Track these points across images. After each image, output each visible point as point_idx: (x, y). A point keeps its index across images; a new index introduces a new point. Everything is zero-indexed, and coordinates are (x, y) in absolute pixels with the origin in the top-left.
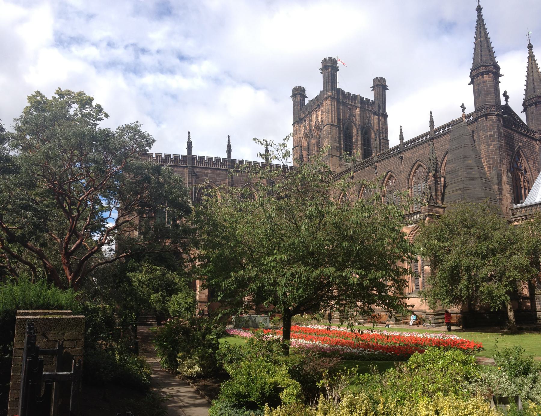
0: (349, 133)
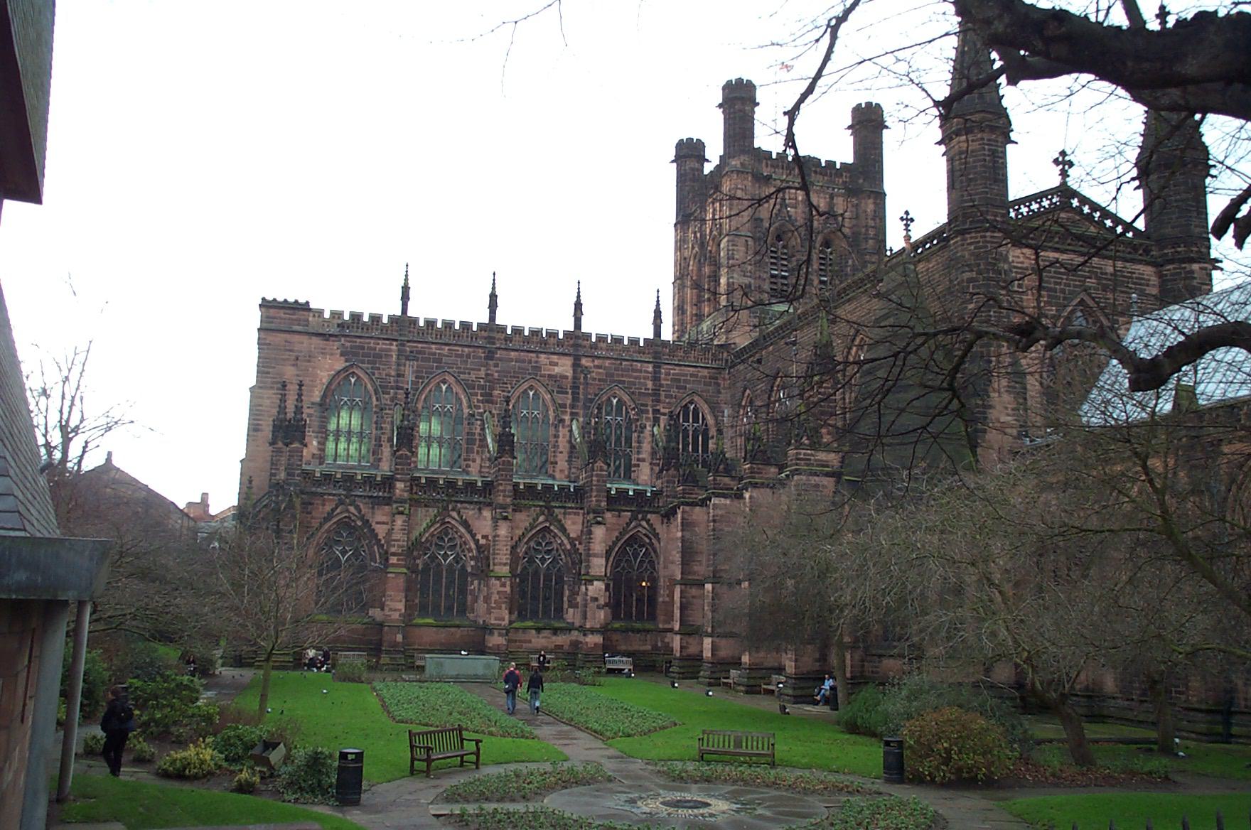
0: (784, 247)
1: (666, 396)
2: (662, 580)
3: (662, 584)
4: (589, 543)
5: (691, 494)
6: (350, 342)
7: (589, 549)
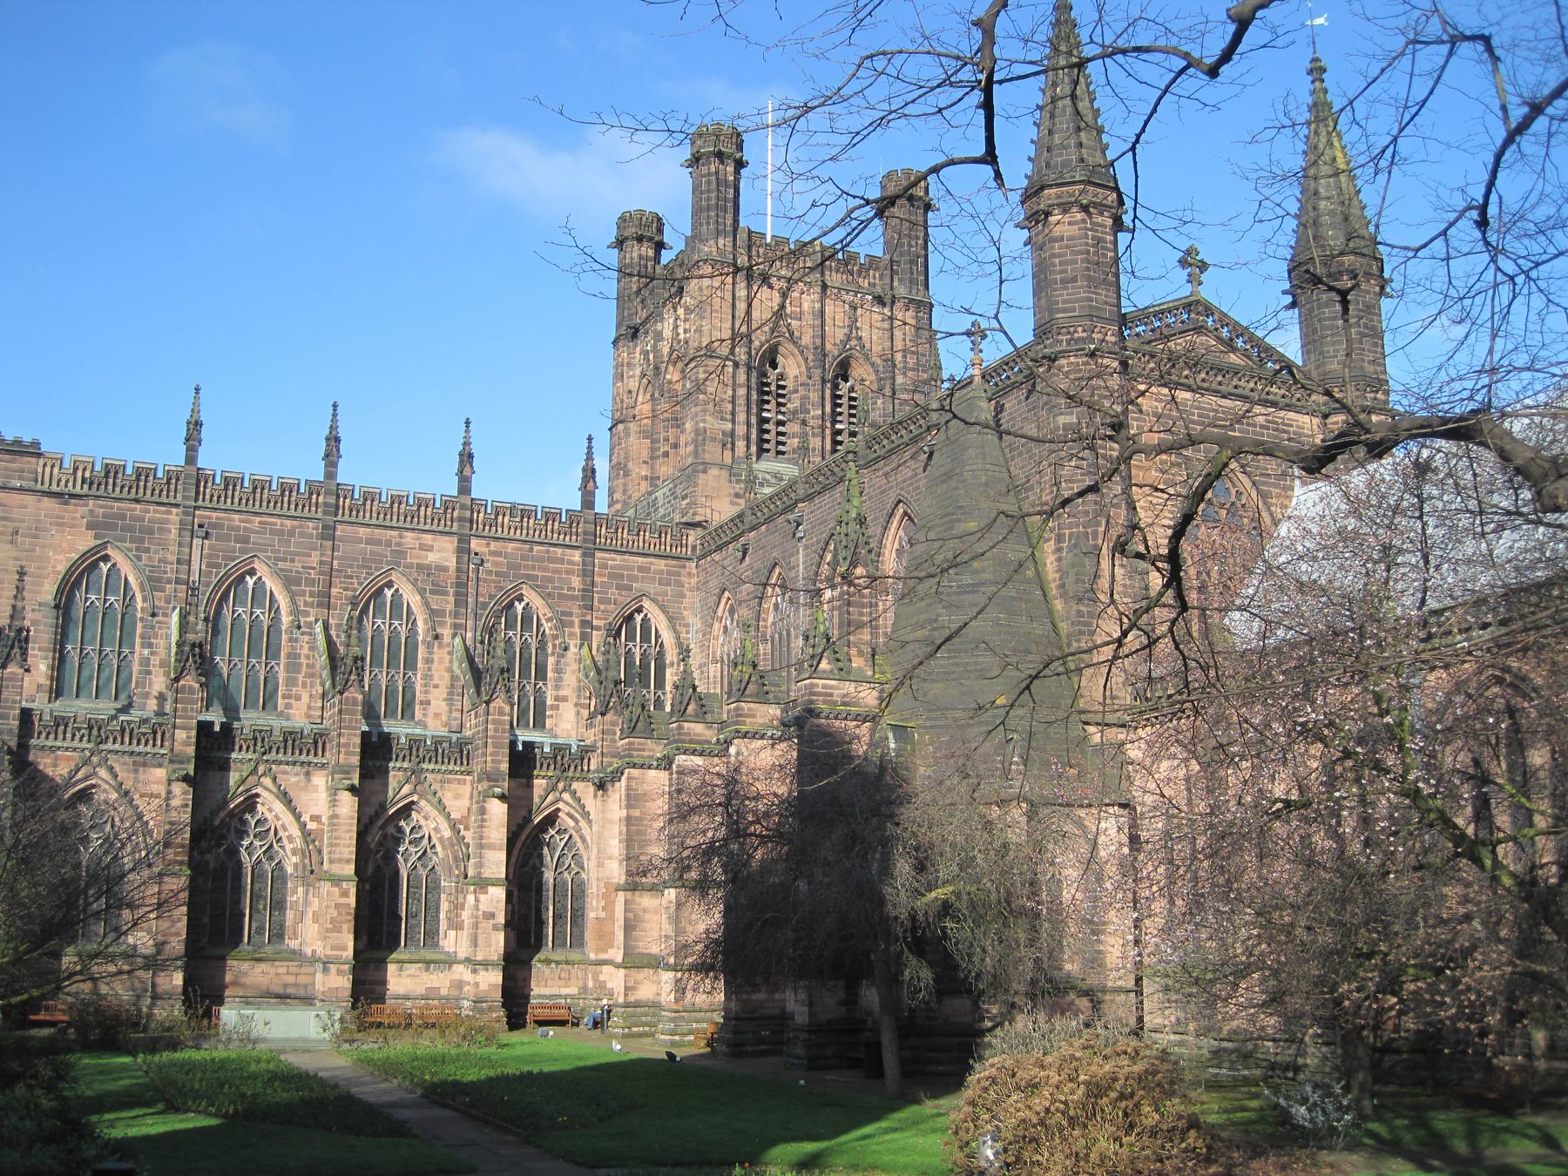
1: (601, 601)
2: (594, 885)
3: (594, 890)
4: (482, 827)
5: (644, 750)
6: (103, 507)
7: (481, 838)
